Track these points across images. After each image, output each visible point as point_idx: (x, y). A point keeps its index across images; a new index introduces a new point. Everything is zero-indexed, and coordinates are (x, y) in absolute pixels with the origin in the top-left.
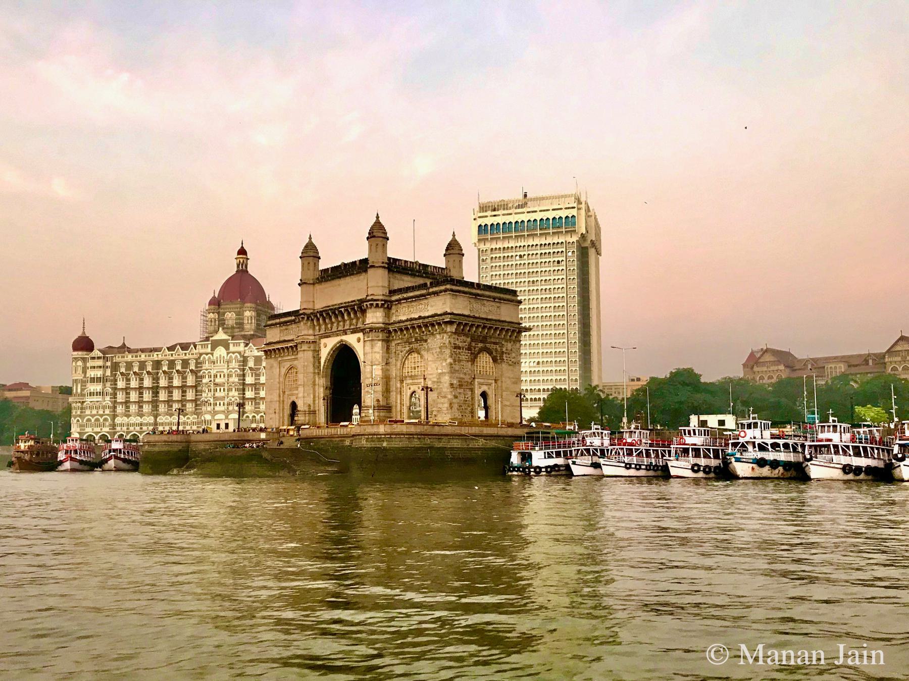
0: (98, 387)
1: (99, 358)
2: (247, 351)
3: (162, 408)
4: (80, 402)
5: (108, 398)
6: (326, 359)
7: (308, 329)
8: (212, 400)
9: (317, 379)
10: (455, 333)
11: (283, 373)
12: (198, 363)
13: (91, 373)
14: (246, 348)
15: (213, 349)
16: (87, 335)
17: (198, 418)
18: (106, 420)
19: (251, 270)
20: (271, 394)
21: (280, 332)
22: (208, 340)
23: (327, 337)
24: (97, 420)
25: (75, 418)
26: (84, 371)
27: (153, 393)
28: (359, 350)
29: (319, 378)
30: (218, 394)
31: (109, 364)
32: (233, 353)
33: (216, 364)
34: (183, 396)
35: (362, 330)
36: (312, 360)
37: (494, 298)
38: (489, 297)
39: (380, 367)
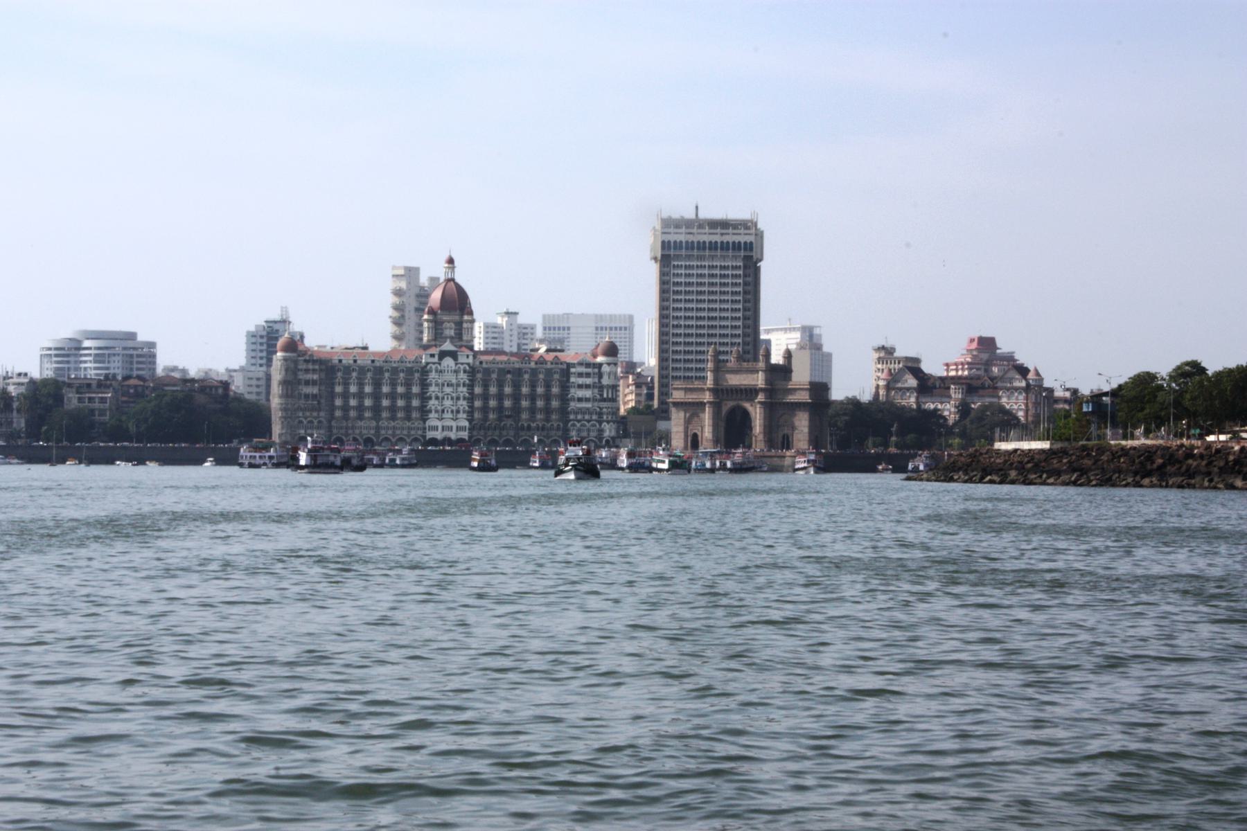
3: (385, 414)
12: (424, 371)
13: (302, 376)
18: (320, 422)
19: (459, 280)
23: (727, 400)
24: (311, 422)
31: (323, 367)
32: (462, 364)
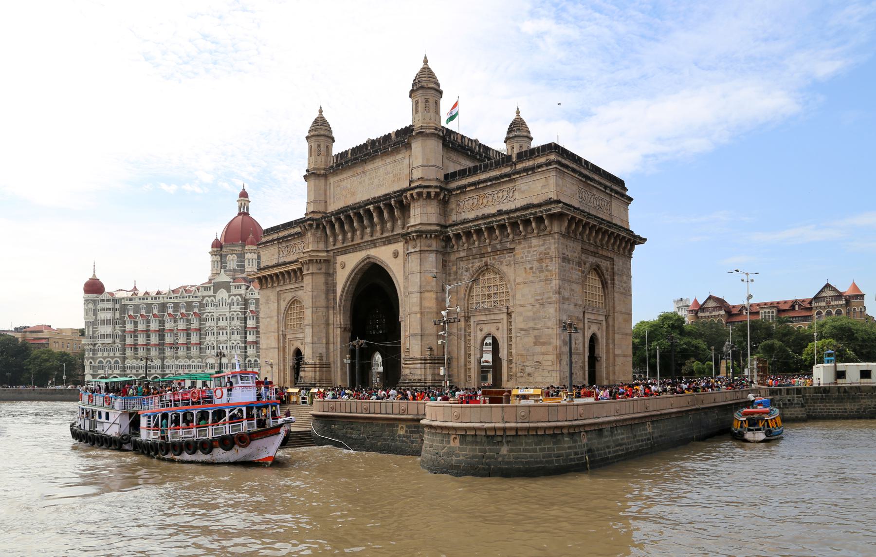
0: (108, 330)
1: (108, 300)
2: (248, 294)
4: (92, 344)
5: (118, 341)
6: (345, 285)
7: (318, 242)
8: (215, 343)
9: (331, 317)
10: (563, 236)
11: (282, 309)
12: (202, 306)
13: (102, 316)
14: (248, 291)
15: (215, 292)
16: (98, 278)
17: (202, 361)
18: (116, 362)
19: (253, 214)
20: (268, 338)
21: (279, 251)
22: (211, 283)
25: (88, 361)
26: (95, 314)
27: (159, 336)
28: (396, 269)
29: (334, 314)
30: (222, 338)
31: (118, 306)
32: (235, 295)
33: (218, 307)
34: (187, 339)
35: (406, 237)
36: (323, 287)
37: (606, 187)
38: (600, 184)
39: (433, 295)
